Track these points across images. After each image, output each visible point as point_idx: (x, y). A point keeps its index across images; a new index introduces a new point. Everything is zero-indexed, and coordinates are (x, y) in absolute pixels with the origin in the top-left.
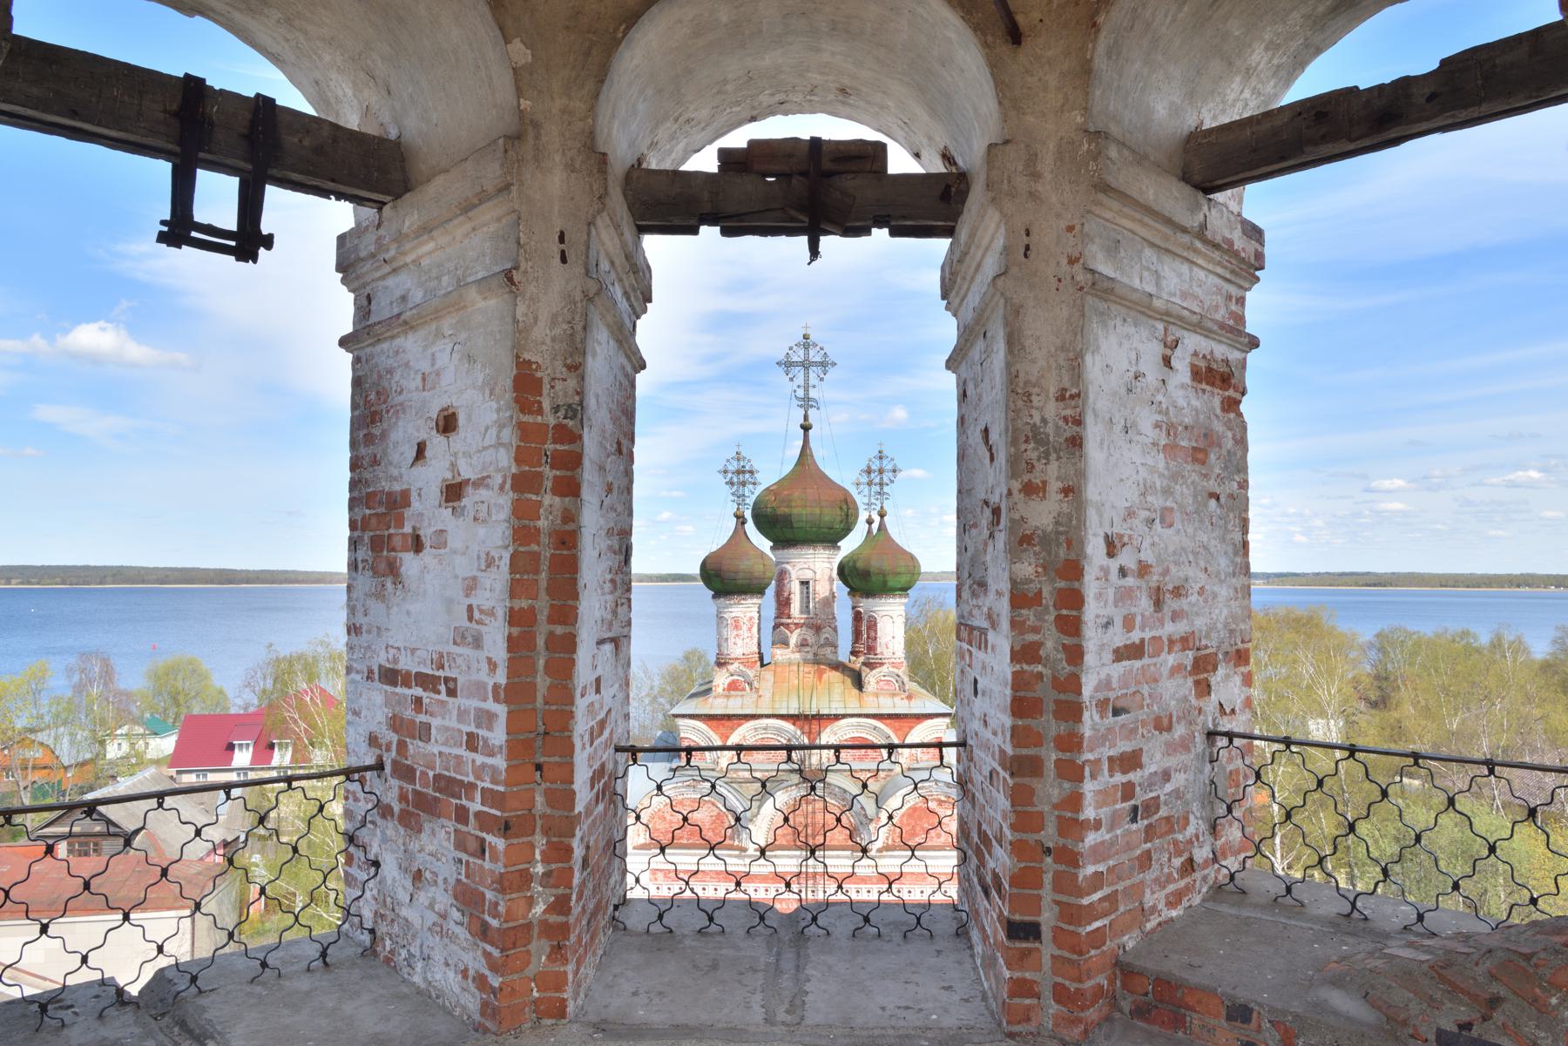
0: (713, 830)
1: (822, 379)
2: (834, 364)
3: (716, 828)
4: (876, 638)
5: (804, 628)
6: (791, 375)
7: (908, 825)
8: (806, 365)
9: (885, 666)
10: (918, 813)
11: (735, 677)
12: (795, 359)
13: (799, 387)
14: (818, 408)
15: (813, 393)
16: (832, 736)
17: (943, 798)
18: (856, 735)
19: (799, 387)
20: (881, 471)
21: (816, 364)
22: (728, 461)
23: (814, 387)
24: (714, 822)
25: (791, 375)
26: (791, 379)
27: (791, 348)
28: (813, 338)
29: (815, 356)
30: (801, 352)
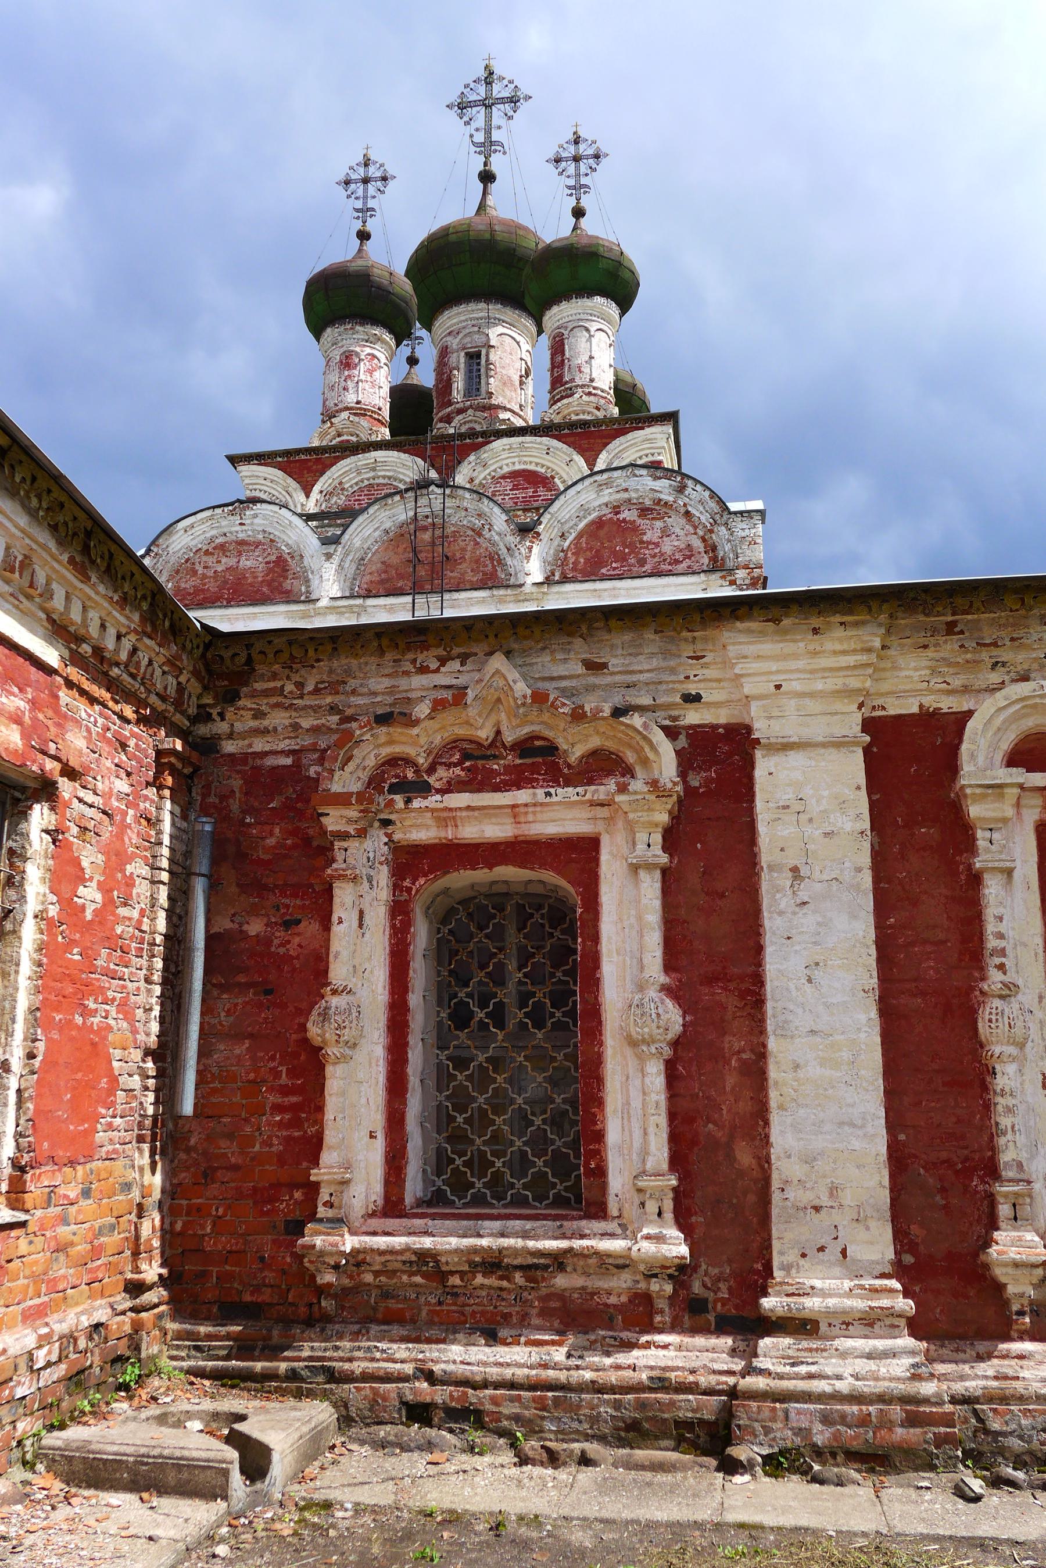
0: (269, 584)
1: (510, 118)
2: (528, 98)
3: (273, 580)
4: (563, 361)
5: (470, 412)
6: (466, 119)
7: (591, 549)
8: (487, 104)
9: (576, 396)
10: (606, 529)
11: (345, 438)
12: (473, 97)
13: (477, 130)
14: (505, 153)
15: (496, 136)
16: (479, 469)
17: (648, 503)
18: (518, 467)
19: (477, 130)
20: (577, 159)
21: (502, 101)
22: (351, 168)
23: (499, 127)
24: (270, 571)
25: (466, 119)
26: (467, 123)
27: (466, 86)
28: (498, 71)
29: (499, 90)
30: (482, 90)
